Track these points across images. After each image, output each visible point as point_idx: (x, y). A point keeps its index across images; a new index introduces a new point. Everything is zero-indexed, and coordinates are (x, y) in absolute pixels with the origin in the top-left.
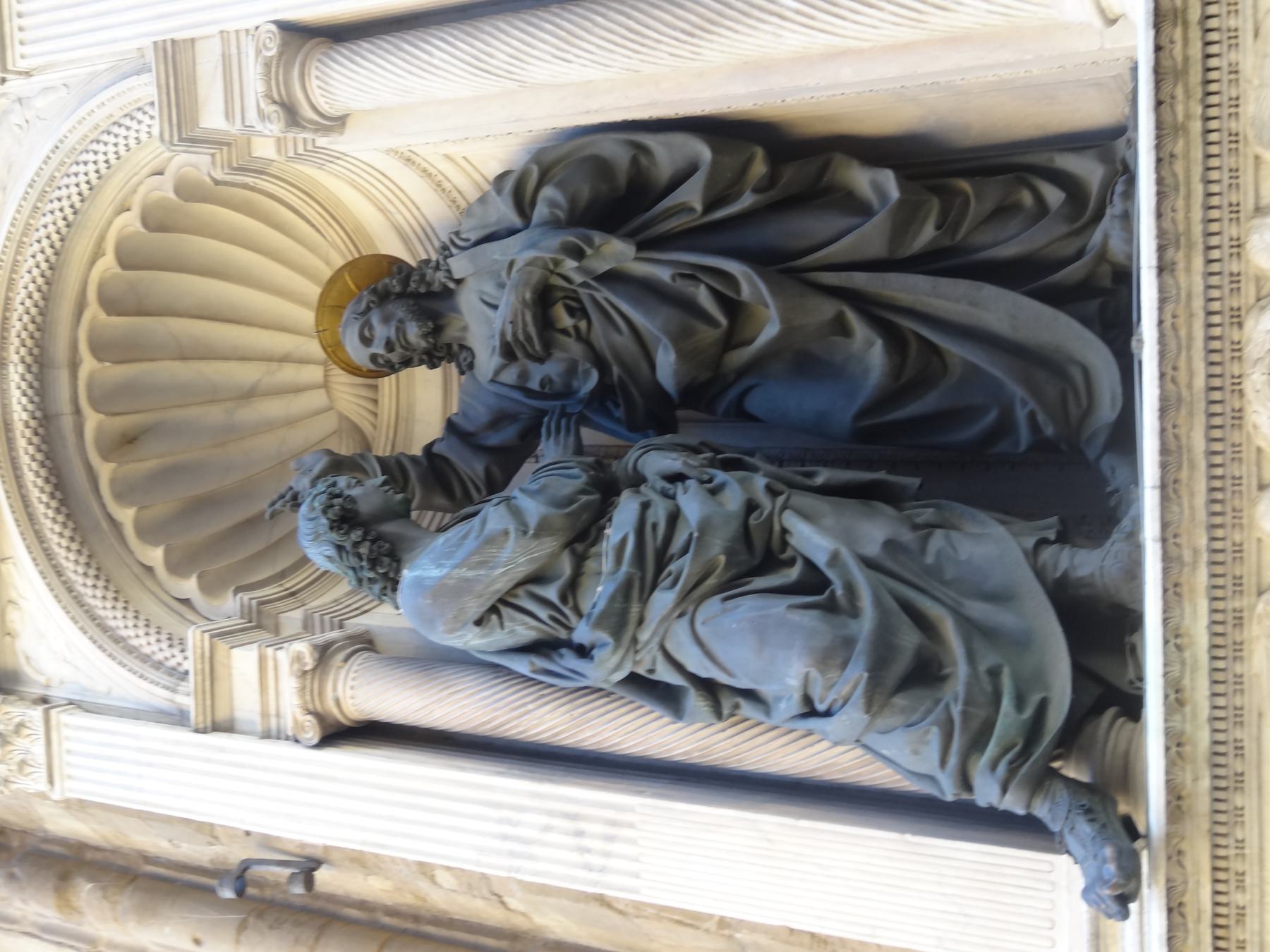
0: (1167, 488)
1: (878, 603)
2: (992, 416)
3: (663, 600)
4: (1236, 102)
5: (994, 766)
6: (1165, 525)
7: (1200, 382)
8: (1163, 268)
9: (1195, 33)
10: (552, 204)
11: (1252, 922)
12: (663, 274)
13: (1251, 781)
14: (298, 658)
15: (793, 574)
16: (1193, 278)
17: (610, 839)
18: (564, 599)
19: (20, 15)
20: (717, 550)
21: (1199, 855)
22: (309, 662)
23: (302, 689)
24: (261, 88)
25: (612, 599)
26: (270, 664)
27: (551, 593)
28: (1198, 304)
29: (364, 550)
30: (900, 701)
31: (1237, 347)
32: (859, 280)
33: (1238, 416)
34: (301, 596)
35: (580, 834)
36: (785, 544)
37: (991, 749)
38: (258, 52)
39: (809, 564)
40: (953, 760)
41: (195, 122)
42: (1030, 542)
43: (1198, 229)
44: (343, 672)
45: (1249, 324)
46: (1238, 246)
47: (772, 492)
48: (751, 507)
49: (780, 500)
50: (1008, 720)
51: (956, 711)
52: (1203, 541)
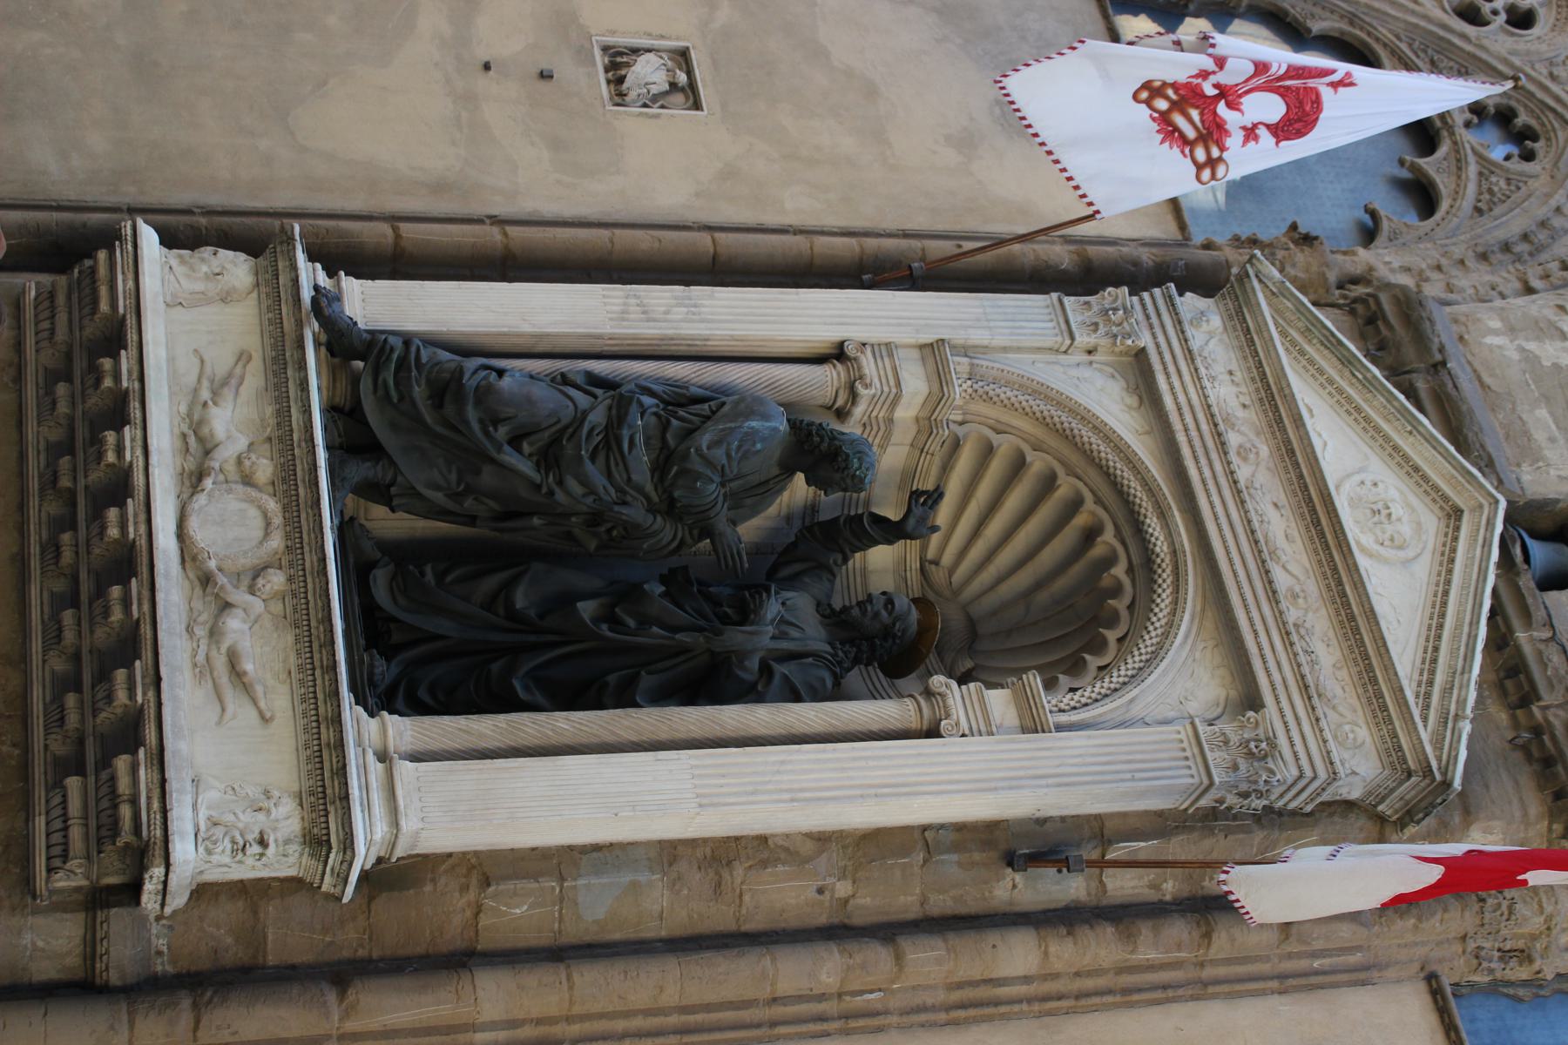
0: (314, 467)
1: (466, 423)
2: (449, 579)
3: (597, 417)
4: (297, 641)
5: (392, 350)
6: (314, 453)
7: (303, 516)
8: (323, 559)
9: (317, 664)
10: (745, 669)
11: (264, 306)
12: (655, 629)
13: (268, 361)
14: (866, 386)
15: (526, 448)
16: (310, 559)
17: (623, 312)
18: (668, 422)
19: (1187, 758)
20: (569, 449)
21: (289, 324)
22: (858, 385)
23: (859, 368)
24: (950, 701)
25: (626, 414)
26: (892, 383)
27: (674, 422)
28: (306, 549)
29: (817, 439)
30: (447, 375)
31: (287, 536)
32: (532, 638)
33: (285, 509)
34: (917, 453)
35: (644, 312)
36: (538, 464)
37: (395, 356)
38: (958, 724)
39: (519, 450)
40: (413, 349)
41: (1015, 693)
42: (399, 479)
43: (309, 580)
44: (836, 383)
45: (282, 546)
46: (290, 579)
47: (551, 493)
48: (560, 483)
49: (544, 490)
50: (389, 376)
51: (414, 373)
52: (296, 451)
